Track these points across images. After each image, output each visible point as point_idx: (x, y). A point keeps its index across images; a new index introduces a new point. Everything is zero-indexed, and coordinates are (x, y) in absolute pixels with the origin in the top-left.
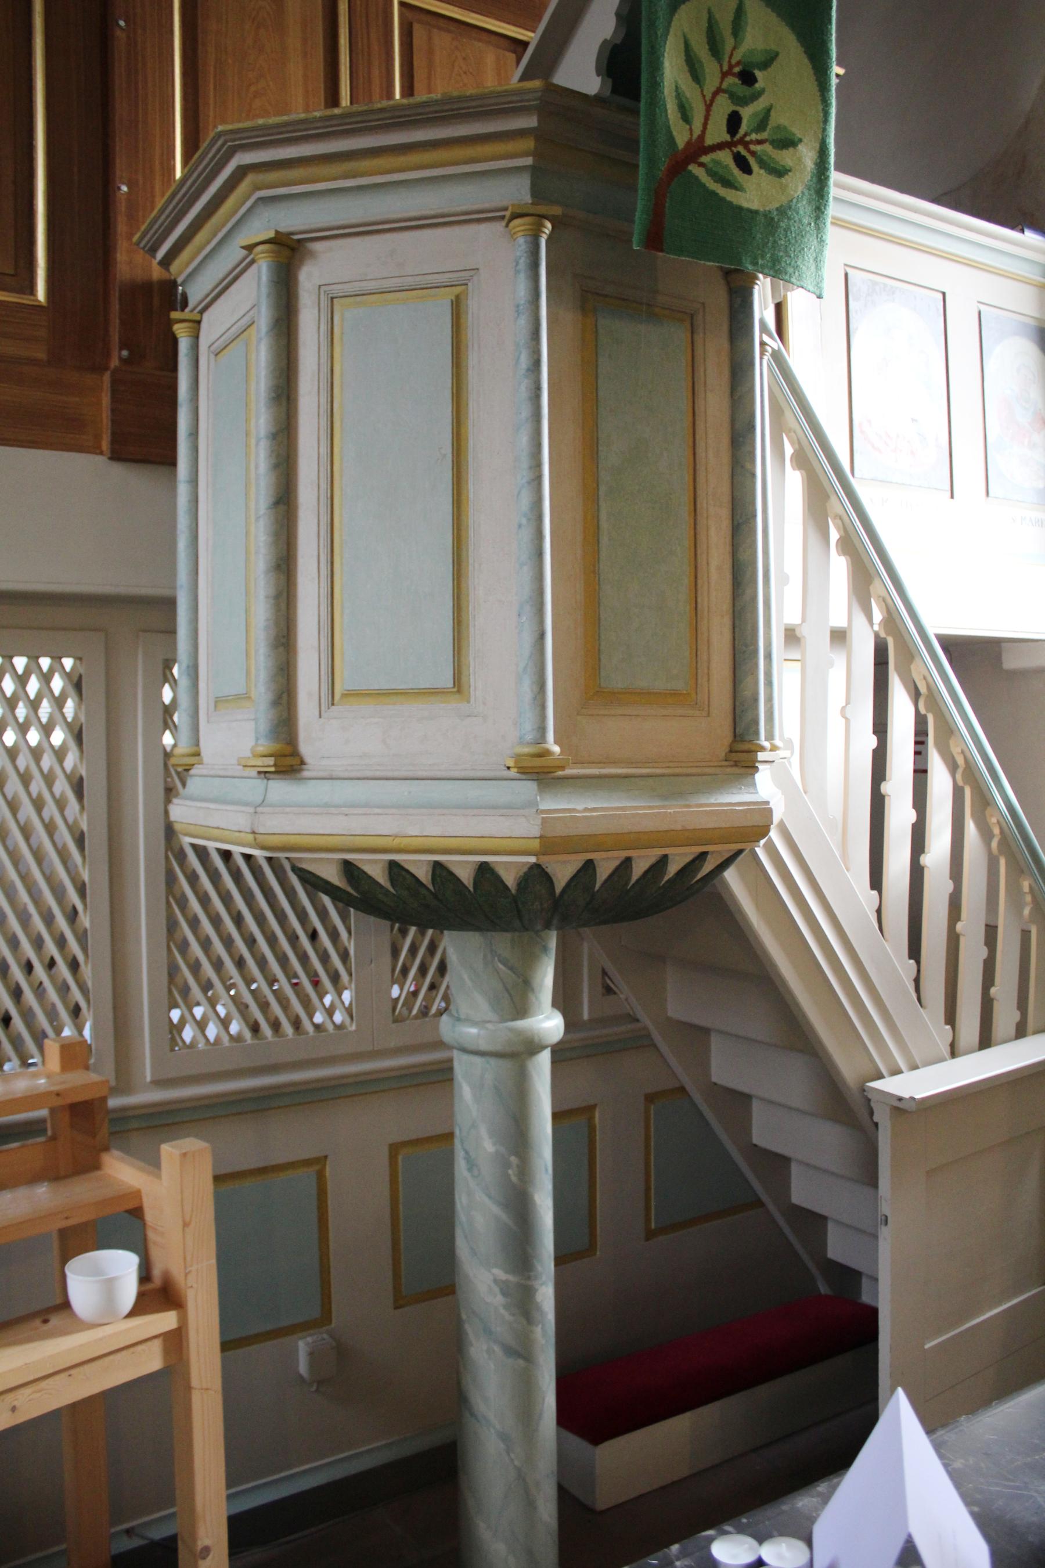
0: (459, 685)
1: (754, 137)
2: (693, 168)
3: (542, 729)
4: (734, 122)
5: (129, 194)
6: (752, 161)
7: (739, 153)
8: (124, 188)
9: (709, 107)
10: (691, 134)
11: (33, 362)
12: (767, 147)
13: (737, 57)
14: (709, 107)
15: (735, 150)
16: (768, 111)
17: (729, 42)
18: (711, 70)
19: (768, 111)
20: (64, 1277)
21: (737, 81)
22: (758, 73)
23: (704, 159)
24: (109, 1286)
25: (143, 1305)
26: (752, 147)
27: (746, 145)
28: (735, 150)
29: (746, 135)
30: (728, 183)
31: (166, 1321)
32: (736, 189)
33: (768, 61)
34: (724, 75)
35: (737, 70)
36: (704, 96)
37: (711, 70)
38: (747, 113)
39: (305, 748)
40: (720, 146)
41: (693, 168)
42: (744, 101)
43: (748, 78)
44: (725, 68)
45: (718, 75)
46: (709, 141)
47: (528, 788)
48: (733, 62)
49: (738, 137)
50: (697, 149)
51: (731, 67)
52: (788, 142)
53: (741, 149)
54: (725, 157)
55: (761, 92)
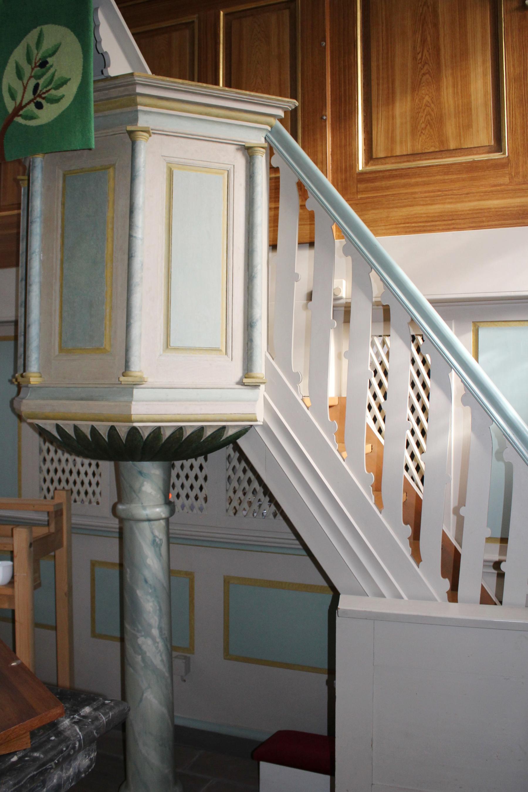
1: (44, 90)
2: (19, 120)
6: (43, 102)
7: (37, 101)
9: (25, 88)
10: (16, 104)
12: (53, 92)
13: (40, 55)
14: (25, 88)
15: (35, 101)
16: (53, 75)
17: (35, 52)
18: (27, 70)
19: (53, 75)
21: (39, 68)
22: (49, 60)
23: (21, 112)
26: (43, 96)
27: (40, 96)
28: (35, 101)
29: (41, 91)
30: (32, 118)
32: (35, 118)
34: (33, 69)
35: (38, 64)
36: (23, 84)
37: (27, 70)
38: (41, 82)
41: (19, 120)
43: (43, 64)
44: (33, 65)
45: (30, 70)
46: (24, 103)
48: (36, 61)
49: (37, 95)
51: (36, 63)
52: (64, 82)
53: (39, 99)
54: (32, 106)
55: (51, 66)
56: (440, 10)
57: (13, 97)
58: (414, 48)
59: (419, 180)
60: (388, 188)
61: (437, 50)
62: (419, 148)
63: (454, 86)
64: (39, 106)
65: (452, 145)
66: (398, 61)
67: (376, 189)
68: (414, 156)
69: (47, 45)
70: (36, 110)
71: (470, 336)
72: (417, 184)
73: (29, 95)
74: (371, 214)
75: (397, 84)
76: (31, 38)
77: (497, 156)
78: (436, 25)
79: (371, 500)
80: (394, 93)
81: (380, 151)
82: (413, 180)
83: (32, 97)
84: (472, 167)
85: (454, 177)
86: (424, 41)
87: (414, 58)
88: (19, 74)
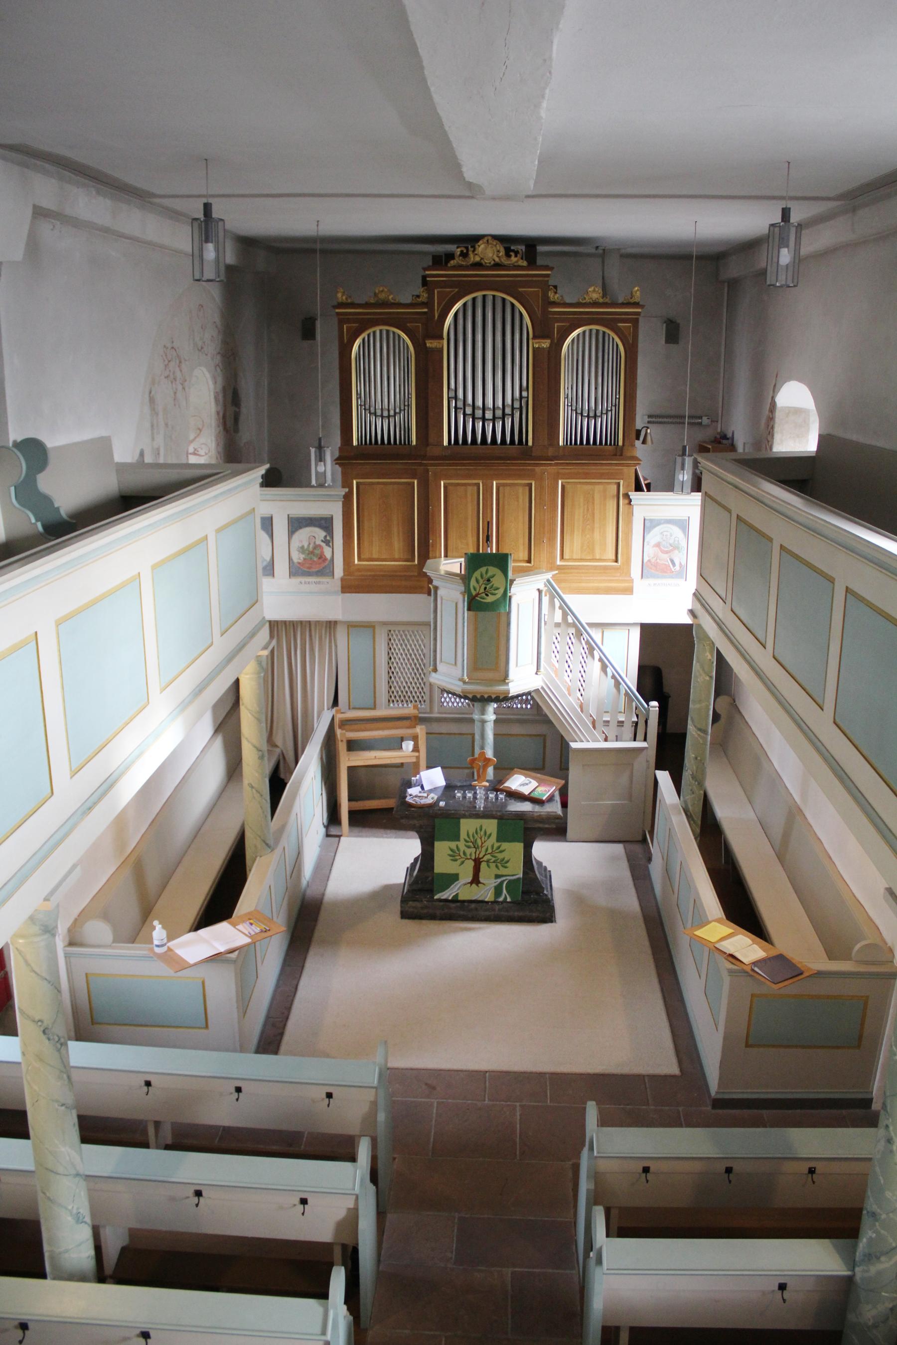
0: (456, 663)
2: (477, 598)
3: (463, 675)
4: (485, 588)
5: (432, 542)
8: (431, 541)
11: (414, 576)
16: (493, 585)
17: (485, 575)
18: (481, 581)
19: (493, 585)
20: (402, 745)
24: (407, 747)
25: (413, 751)
30: (484, 599)
31: (417, 754)
33: (493, 576)
37: (481, 581)
38: (488, 587)
39: (438, 668)
40: (482, 593)
42: (487, 585)
43: (489, 580)
47: (461, 683)
50: (477, 595)
52: (497, 589)
54: (484, 595)
56: (595, 497)
57: (475, 589)
58: (584, 512)
59: (583, 571)
60: (571, 573)
61: (593, 514)
62: (584, 557)
63: (600, 532)
64: (487, 595)
65: (598, 558)
66: (576, 517)
67: (564, 573)
68: (581, 560)
69: (490, 574)
70: (485, 596)
71: (600, 634)
72: (583, 573)
73: (482, 590)
74: (563, 585)
75: (575, 527)
76: (483, 569)
77: (616, 564)
78: (593, 503)
79: (579, 710)
80: (574, 531)
81: (566, 556)
82: (581, 571)
83: (483, 591)
84: (605, 568)
85: (599, 571)
86: (588, 510)
87: (583, 517)
88: (477, 581)
